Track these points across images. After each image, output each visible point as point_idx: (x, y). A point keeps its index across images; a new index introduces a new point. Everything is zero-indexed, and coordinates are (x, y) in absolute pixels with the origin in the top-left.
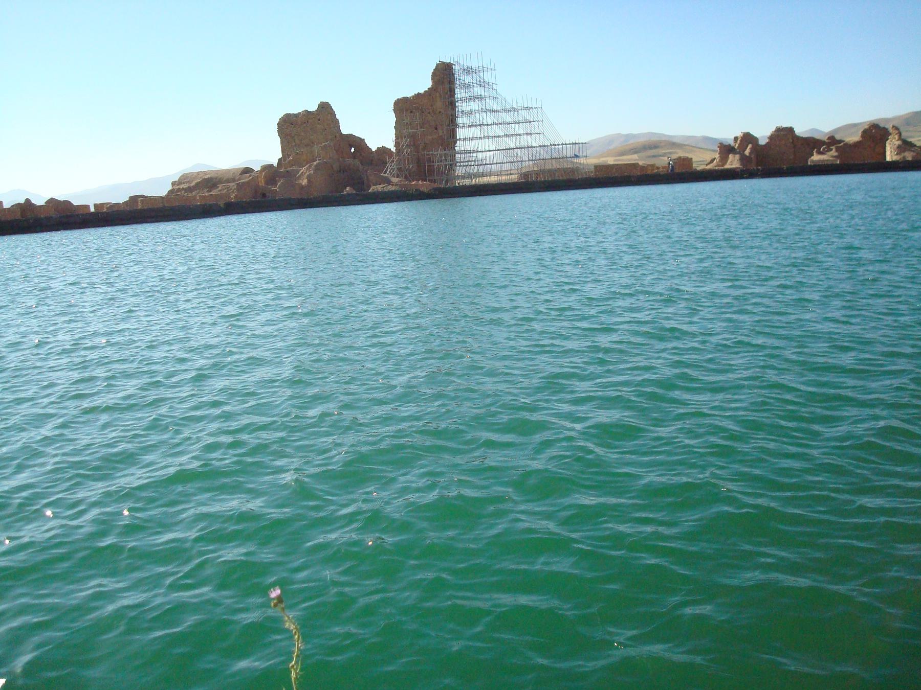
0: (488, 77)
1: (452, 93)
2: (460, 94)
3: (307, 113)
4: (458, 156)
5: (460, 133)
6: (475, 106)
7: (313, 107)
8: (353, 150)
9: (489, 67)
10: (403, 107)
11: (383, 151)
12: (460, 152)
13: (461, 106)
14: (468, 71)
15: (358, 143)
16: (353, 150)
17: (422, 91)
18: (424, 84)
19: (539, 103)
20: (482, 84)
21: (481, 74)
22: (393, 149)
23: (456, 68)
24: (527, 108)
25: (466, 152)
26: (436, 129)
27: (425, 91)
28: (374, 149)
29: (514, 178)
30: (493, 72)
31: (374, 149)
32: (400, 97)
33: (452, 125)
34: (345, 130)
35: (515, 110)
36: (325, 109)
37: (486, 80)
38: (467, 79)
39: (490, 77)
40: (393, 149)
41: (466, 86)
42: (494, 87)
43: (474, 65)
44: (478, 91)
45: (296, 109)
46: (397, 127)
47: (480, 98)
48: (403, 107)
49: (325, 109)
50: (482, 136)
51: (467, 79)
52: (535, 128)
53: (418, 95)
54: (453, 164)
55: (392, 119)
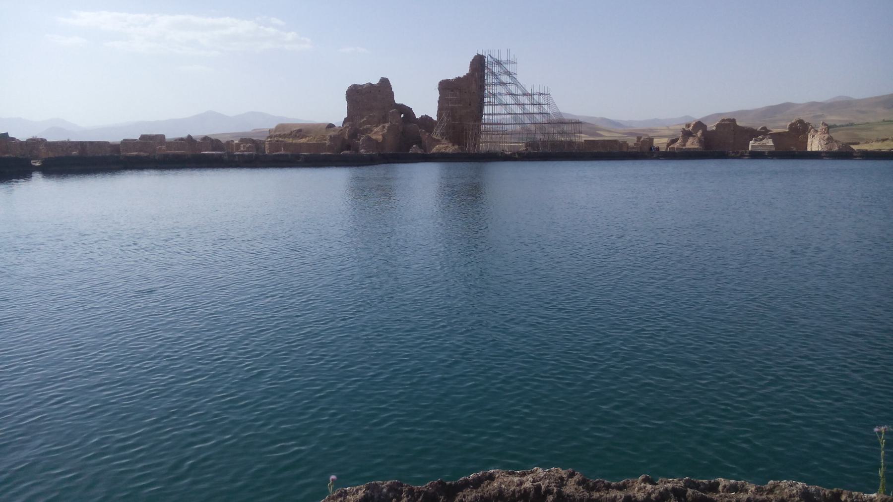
0: (509, 68)
2: (489, 79)
3: (371, 85)
4: (483, 127)
5: (486, 110)
6: (501, 89)
7: (375, 81)
8: (402, 116)
9: (513, 61)
10: (446, 87)
11: (426, 119)
13: (488, 90)
14: (498, 63)
15: (407, 111)
16: (402, 116)
17: (462, 76)
18: (462, 69)
20: (508, 74)
22: (435, 118)
24: (541, 94)
25: (488, 124)
26: (470, 105)
27: (464, 76)
28: (418, 116)
29: (522, 147)
31: (418, 116)
32: (444, 78)
33: (481, 105)
34: (398, 100)
35: (531, 95)
36: (385, 84)
39: (511, 67)
40: (435, 118)
41: (493, 74)
43: (504, 59)
44: (504, 78)
45: (362, 81)
46: (441, 101)
47: (504, 84)
48: (446, 87)
49: (385, 84)
50: (506, 113)
51: (496, 69)
52: (546, 109)
53: (458, 79)
54: (478, 132)
55: (437, 95)
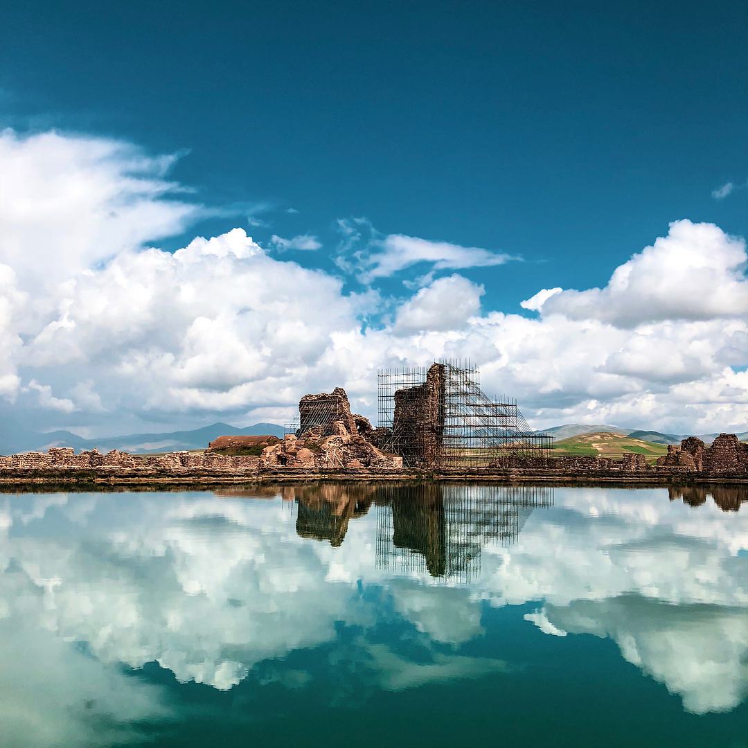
0: (472, 377)
1: (442, 389)
2: (449, 389)
5: (447, 422)
6: (462, 400)
7: (329, 391)
8: (358, 428)
12: (446, 437)
14: (458, 371)
19: (514, 401)
21: (468, 375)
23: (447, 368)
30: (477, 374)
37: (471, 380)
38: (454, 378)
42: (478, 386)
44: (464, 388)
